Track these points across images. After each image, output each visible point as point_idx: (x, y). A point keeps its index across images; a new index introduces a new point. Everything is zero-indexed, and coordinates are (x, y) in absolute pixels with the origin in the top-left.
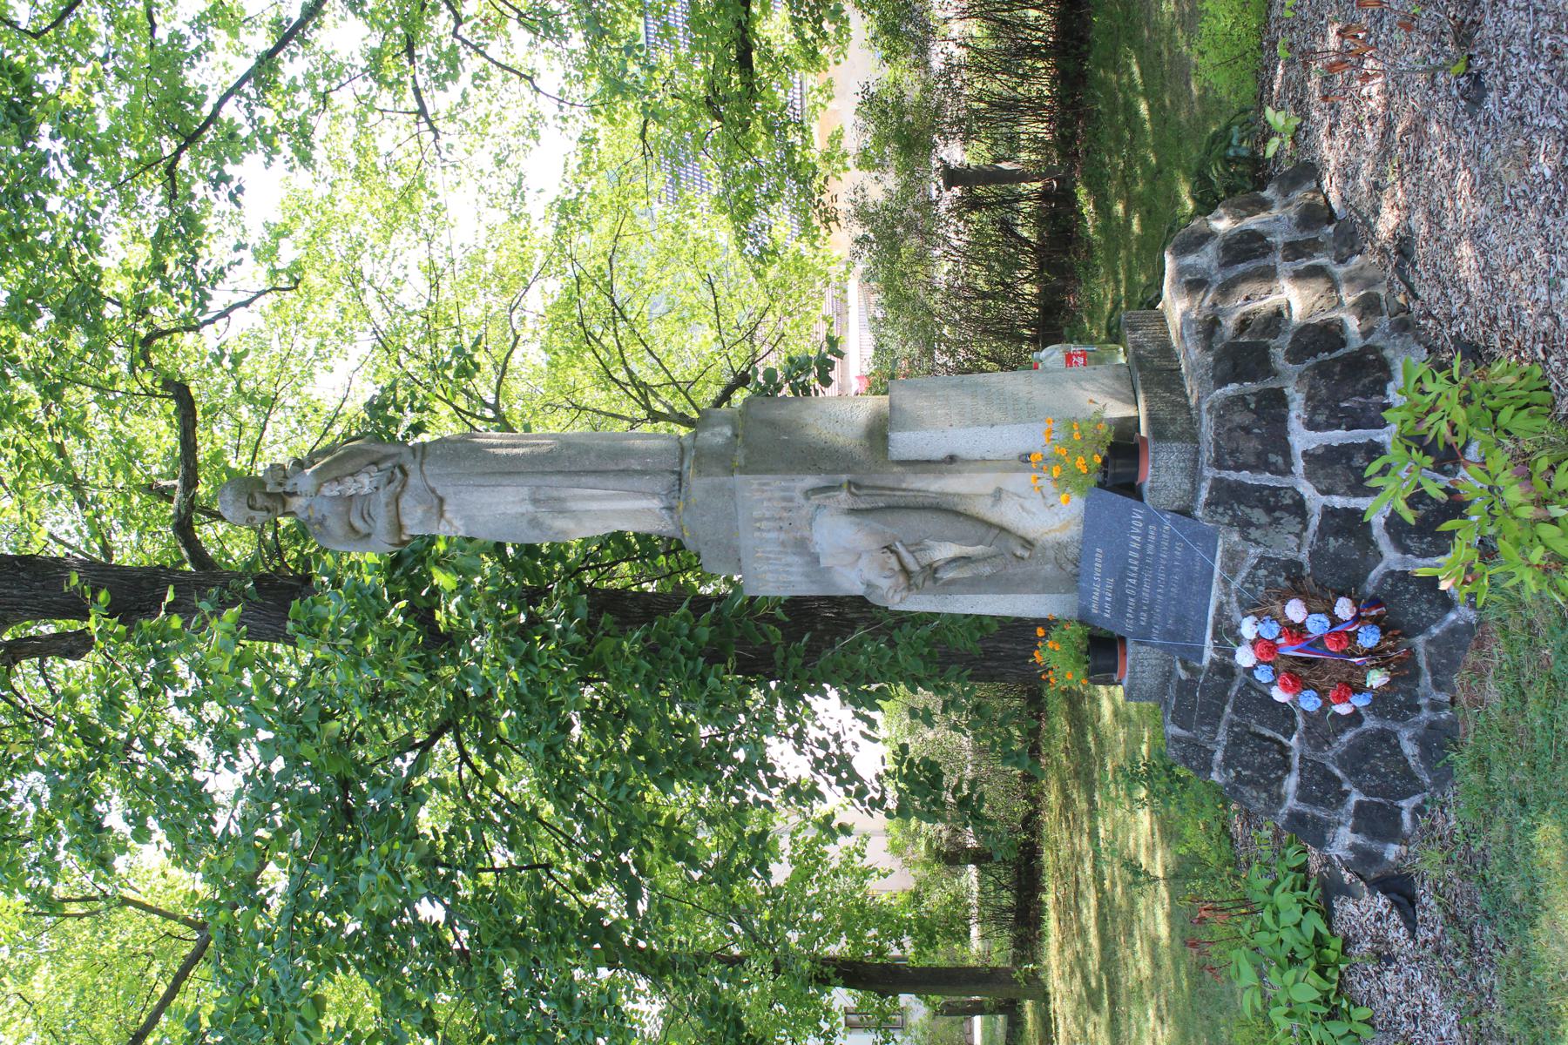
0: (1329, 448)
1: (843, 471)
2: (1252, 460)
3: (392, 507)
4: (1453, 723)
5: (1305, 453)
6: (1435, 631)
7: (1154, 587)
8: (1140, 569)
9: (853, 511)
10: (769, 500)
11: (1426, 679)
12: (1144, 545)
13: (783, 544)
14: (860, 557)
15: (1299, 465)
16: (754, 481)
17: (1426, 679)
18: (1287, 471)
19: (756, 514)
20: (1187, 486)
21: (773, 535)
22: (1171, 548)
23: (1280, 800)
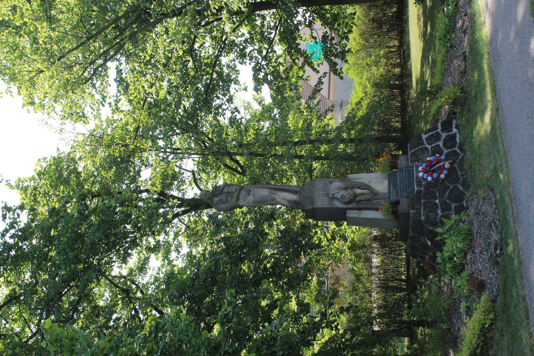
0: (429, 136)
5: (426, 139)
6: (458, 161)
7: (403, 185)
13: (323, 194)
15: (425, 142)
17: (460, 173)
18: (423, 144)
19: (318, 187)
23: (438, 214)
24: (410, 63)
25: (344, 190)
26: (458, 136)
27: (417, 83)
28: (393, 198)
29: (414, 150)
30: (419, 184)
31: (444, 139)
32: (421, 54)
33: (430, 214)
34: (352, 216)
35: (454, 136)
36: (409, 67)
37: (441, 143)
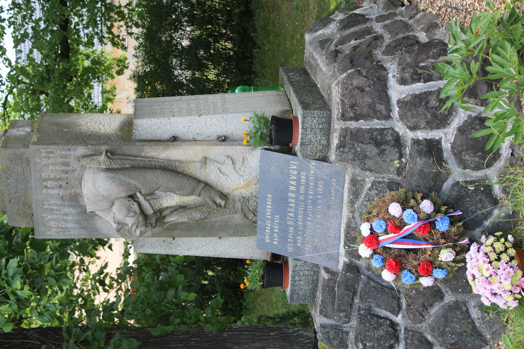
1: (103, 144)
8: (297, 205)
9: (108, 170)
10: (53, 164)
12: (298, 187)
13: (62, 198)
14: (113, 204)
15: (396, 110)
16: (43, 150)
18: (388, 117)
19: (44, 175)
20: (324, 142)
21: (55, 192)
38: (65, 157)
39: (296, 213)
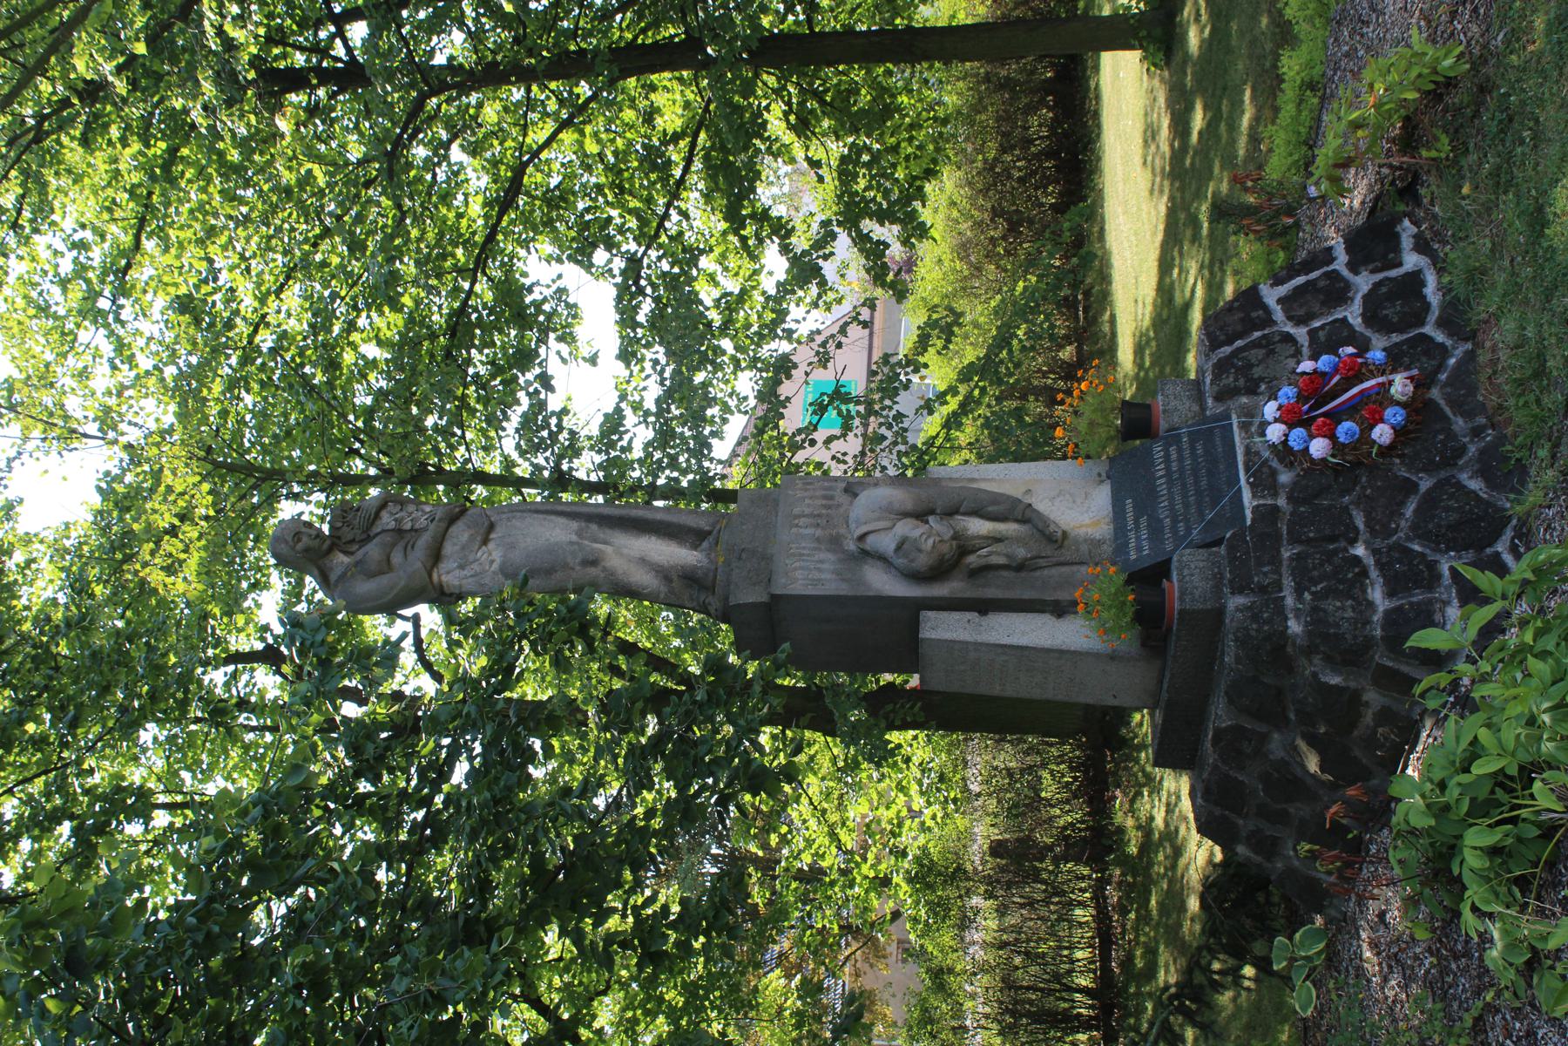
0: (1297, 289)
2: (1239, 328)
3: (443, 525)
4: (1501, 439)
5: (1279, 301)
6: (1443, 377)
7: (1185, 496)
11: (1459, 423)
12: (1168, 468)
13: (818, 540)
15: (1278, 314)
17: (1459, 423)
18: (1269, 321)
19: (796, 511)
20: (1196, 408)
22: (1193, 449)
23: (1371, 605)
24: (1106, 316)
25: (910, 522)
26: (1431, 280)
27: (1139, 351)
28: (1140, 550)
29: (1227, 350)
30: (1264, 481)
31: (1366, 298)
32: (1160, 237)
33: (1331, 605)
34: (948, 636)
35: (1414, 280)
36: (1106, 328)
37: (1353, 314)
38: (830, 488)
39: (1171, 499)
